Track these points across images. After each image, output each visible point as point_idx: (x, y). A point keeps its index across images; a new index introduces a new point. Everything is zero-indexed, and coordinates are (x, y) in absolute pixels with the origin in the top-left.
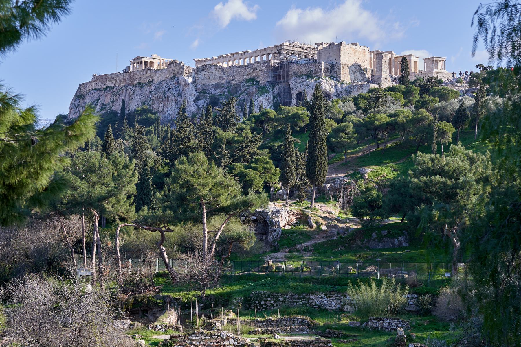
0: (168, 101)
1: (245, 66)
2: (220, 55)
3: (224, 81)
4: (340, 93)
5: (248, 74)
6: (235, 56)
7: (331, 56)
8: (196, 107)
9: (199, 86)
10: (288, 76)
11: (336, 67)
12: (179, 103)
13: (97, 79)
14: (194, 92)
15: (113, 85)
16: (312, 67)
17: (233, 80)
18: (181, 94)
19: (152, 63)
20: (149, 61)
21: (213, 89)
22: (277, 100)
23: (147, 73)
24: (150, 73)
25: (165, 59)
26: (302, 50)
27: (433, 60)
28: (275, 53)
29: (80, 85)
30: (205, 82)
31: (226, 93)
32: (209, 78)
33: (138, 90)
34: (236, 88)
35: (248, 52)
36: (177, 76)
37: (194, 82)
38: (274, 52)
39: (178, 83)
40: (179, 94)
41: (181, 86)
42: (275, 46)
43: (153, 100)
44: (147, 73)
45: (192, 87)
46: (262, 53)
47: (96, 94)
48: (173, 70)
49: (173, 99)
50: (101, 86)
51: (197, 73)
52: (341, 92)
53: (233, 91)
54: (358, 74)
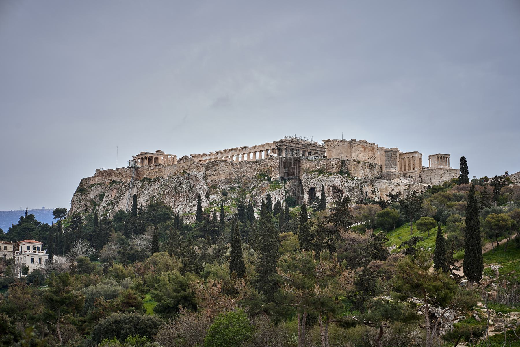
1: (257, 162)
4: (351, 189)
6: (233, 151)
7: (342, 153)
8: (208, 202)
9: (209, 181)
10: (299, 172)
11: (347, 164)
12: (190, 198)
13: (100, 173)
14: (205, 187)
15: (119, 180)
17: (244, 176)
18: (192, 189)
22: (289, 195)
23: (155, 168)
24: (159, 169)
26: (299, 146)
28: (274, 149)
29: (82, 180)
30: (215, 177)
31: (237, 189)
32: (219, 174)
34: (247, 184)
36: (187, 171)
38: (272, 148)
41: (192, 182)
42: (274, 143)
44: (155, 168)
48: (183, 167)
49: (185, 194)
52: (353, 187)
54: (368, 171)
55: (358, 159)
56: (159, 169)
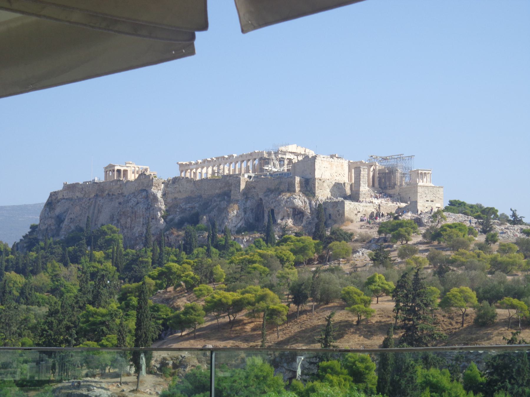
0: (135, 217)
2: (204, 159)
5: (220, 188)
6: (220, 160)
15: (82, 196)
19: (125, 171)
20: (122, 169)
21: (184, 203)
23: (116, 184)
25: (140, 167)
27: (418, 173)
30: (176, 195)
35: (233, 156)
39: (147, 197)
40: (147, 209)
41: (150, 201)
43: (120, 215)
46: (248, 158)
53: (206, 206)
55: (323, 177)
56: (120, 185)
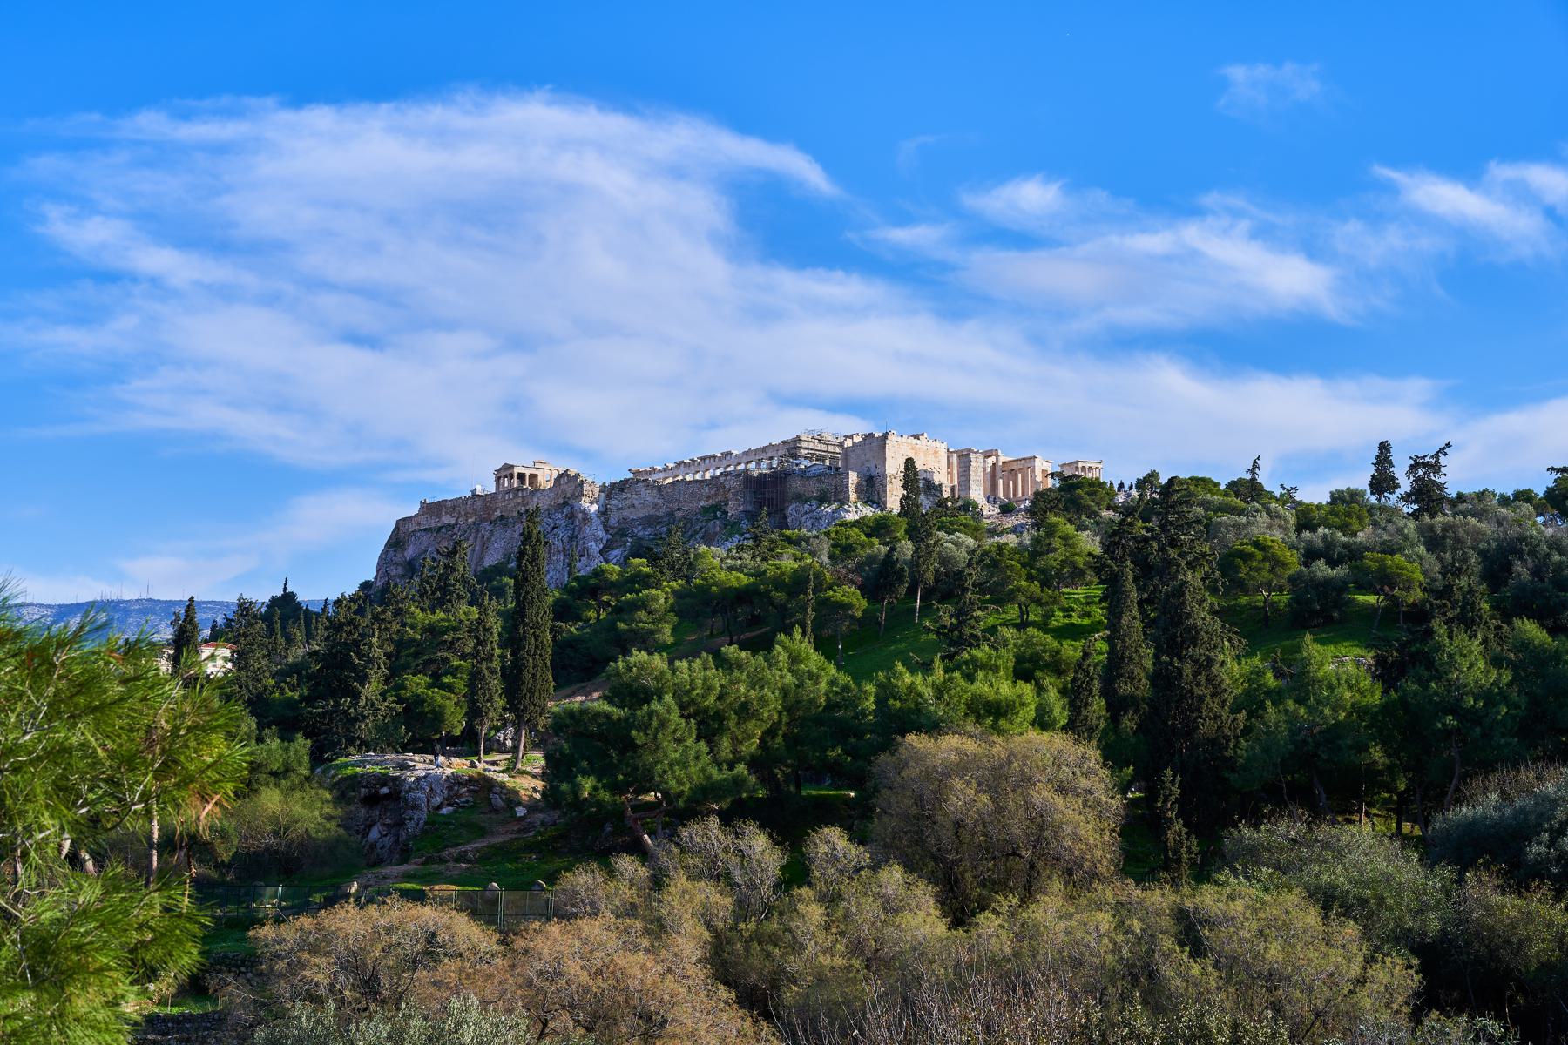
3: (661, 512)
9: (613, 522)
11: (877, 482)
14: (601, 533)
16: (827, 483)
20: (528, 472)
23: (516, 496)
33: (498, 533)
37: (604, 513)
39: (571, 517)
40: (572, 538)
45: (597, 522)
47: (426, 539)
48: (564, 492)
50: (434, 523)
51: (609, 497)
